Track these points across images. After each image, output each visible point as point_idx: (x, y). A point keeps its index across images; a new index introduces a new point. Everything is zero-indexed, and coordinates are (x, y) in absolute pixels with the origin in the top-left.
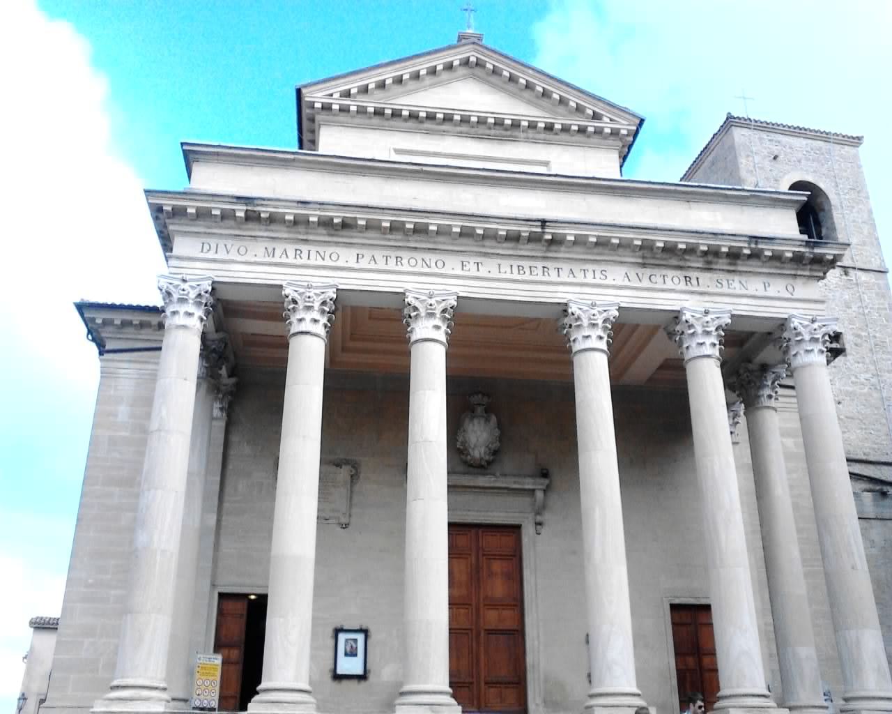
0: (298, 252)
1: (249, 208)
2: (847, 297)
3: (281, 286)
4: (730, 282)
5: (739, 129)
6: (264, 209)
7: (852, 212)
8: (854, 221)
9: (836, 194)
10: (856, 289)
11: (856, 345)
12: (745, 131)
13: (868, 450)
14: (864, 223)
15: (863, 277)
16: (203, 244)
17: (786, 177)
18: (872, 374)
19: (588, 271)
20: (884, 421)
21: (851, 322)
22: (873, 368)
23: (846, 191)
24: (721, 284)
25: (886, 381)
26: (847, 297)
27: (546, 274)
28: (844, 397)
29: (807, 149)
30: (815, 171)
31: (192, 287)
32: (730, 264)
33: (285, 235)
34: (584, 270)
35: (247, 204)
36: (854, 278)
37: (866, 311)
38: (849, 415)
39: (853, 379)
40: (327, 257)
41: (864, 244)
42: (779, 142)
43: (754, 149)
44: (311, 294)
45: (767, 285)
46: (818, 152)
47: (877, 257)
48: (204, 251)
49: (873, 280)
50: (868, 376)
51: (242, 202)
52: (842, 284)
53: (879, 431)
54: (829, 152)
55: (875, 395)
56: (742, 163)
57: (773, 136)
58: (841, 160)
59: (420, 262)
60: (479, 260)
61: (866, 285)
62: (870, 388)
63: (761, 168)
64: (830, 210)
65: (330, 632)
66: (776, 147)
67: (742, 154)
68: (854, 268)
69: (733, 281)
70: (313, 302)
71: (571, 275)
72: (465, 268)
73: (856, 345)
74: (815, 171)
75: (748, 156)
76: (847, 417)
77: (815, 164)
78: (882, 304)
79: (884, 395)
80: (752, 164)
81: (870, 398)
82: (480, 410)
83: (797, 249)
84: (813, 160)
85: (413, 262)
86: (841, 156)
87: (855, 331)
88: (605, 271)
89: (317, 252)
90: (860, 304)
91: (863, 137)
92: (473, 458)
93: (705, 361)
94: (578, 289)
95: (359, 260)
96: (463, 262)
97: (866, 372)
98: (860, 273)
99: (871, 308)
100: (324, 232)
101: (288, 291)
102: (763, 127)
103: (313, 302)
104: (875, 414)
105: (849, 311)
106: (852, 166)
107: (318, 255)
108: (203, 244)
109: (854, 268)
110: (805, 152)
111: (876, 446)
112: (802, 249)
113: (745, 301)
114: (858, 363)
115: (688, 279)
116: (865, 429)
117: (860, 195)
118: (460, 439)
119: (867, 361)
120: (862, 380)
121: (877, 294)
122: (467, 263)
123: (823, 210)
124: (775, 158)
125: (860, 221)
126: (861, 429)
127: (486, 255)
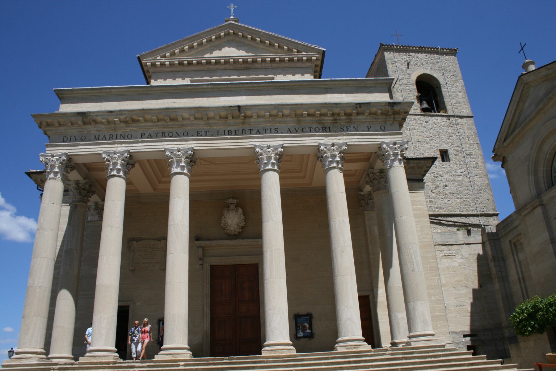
0: (111, 136)
9: (443, 79)
10: (455, 126)
11: (456, 155)
13: (462, 209)
14: (460, 92)
15: (460, 120)
16: (64, 137)
17: (415, 73)
18: (465, 170)
19: (267, 129)
20: (471, 193)
21: (453, 143)
23: (449, 77)
24: (343, 129)
26: (450, 131)
28: (449, 182)
29: (426, 57)
30: (431, 68)
32: (348, 119)
34: (265, 129)
36: (454, 121)
37: (461, 138)
38: (452, 192)
39: (454, 173)
42: (411, 56)
43: (396, 60)
45: (369, 127)
47: (467, 109)
48: (64, 141)
51: (80, 115)
52: (447, 124)
53: (468, 198)
55: (466, 180)
56: (389, 68)
58: (446, 61)
59: (175, 134)
61: (461, 124)
62: (463, 177)
63: (401, 70)
66: (409, 58)
67: (389, 63)
68: (454, 116)
69: (350, 127)
71: (258, 132)
73: (456, 155)
75: (393, 64)
76: (450, 193)
77: (431, 65)
78: (470, 133)
79: (471, 179)
80: (395, 68)
81: (464, 182)
87: (455, 148)
88: (277, 129)
90: (457, 134)
93: (332, 171)
95: (143, 136)
96: (198, 132)
98: (457, 119)
106: (452, 64)
107: (121, 136)
108: (64, 137)
109: (454, 116)
110: (425, 59)
111: (466, 206)
114: (457, 164)
116: (461, 198)
117: (457, 78)
119: (462, 163)
120: (459, 173)
121: (467, 128)
122: (200, 132)
124: (408, 64)
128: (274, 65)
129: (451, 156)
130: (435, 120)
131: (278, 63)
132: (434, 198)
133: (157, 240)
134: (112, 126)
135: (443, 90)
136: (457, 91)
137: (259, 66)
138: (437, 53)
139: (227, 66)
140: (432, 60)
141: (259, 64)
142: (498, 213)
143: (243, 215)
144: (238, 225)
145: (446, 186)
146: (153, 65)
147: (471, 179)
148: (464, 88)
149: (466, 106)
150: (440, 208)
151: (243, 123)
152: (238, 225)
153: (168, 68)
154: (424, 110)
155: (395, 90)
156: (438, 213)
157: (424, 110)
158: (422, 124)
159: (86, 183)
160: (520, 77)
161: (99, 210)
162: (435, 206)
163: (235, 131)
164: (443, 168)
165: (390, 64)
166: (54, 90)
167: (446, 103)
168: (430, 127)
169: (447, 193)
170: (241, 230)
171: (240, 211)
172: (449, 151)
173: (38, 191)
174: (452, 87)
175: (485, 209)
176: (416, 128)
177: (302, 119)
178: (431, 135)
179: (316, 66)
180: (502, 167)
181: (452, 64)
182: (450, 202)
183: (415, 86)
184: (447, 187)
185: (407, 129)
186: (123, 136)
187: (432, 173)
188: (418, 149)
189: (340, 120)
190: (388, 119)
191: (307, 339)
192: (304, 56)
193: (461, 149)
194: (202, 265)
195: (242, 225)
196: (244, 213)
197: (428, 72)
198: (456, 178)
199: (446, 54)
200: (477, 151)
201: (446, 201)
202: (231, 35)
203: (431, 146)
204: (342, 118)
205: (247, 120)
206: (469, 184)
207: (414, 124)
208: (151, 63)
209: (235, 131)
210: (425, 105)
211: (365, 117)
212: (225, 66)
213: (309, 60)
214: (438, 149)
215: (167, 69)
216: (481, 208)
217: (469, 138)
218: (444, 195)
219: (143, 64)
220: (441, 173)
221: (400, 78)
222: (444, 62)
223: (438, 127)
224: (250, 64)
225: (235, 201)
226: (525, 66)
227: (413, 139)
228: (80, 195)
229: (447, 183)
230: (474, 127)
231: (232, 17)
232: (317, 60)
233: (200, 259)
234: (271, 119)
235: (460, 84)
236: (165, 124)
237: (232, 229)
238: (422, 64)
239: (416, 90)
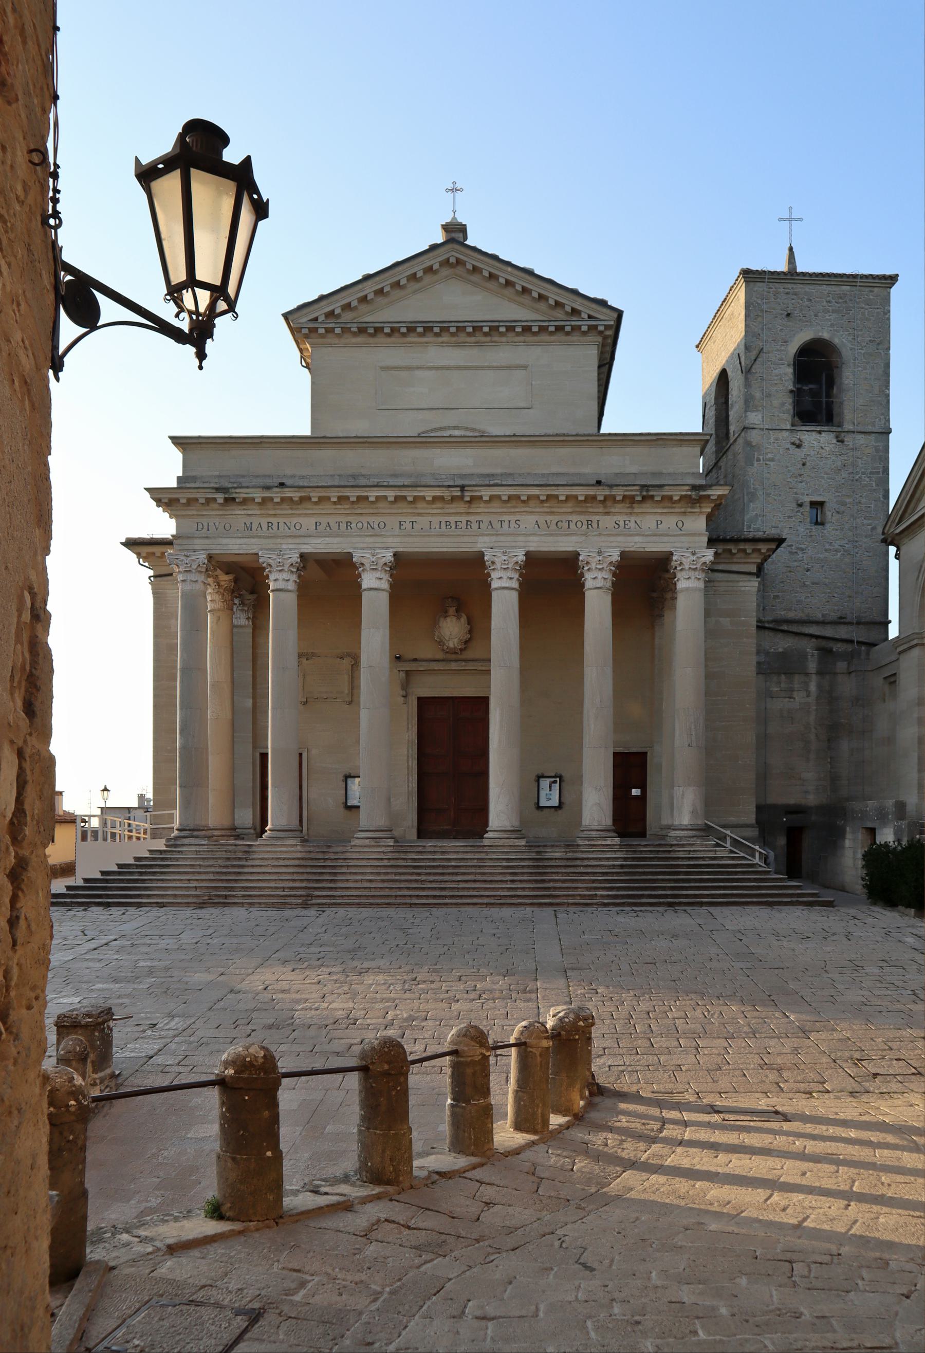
1: (227, 496)
4: (627, 522)
6: (237, 495)
25: (861, 546)
27: (469, 527)
33: (258, 512)
35: (224, 493)
40: (292, 528)
46: (841, 301)
59: (365, 525)
60: (414, 519)
65: (341, 778)
70: (283, 566)
71: (490, 527)
72: (402, 527)
82: (452, 610)
83: (684, 493)
84: (834, 311)
85: (360, 525)
91: (897, 275)
92: (448, 647)
100: (288, 507)
102: (780, 279)
110: (825, 303)
112: (689, 493)
115: (590, 522)
117: (880, 347)
118: (437, 634)
127: (419, 514)
130: (815, 442)
140: (839, 305)
158: (788, 449)
163: (456, 522)
174: (865, 369)
181: (877, 313)
183: (792, 366)
185: (758, 460)
186: (289, 525)
187: (789, 546)
190: (689, 510)
197: (826, 335)
209: (456, 522)
222: (863, 308)
223: (819, 456)
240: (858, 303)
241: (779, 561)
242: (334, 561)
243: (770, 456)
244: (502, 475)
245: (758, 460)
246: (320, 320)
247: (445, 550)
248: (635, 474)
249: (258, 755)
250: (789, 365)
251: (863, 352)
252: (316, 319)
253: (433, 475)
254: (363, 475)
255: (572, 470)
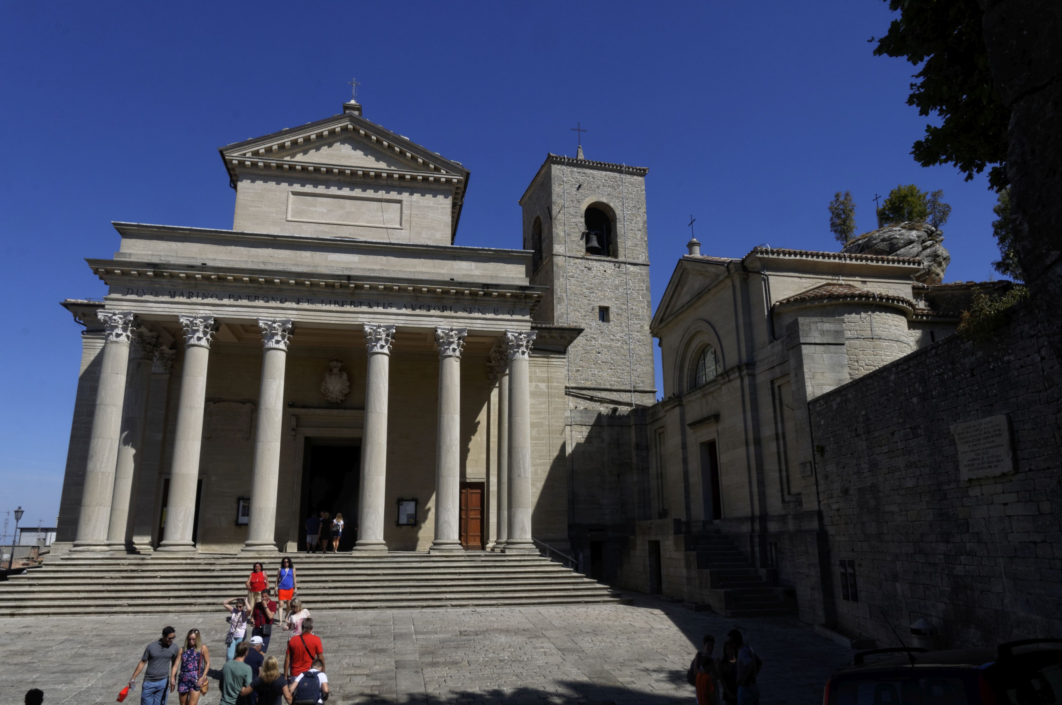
2: (617, 282)
3: (178, 316)
5: (556, 165)
7: (631, 223)
8: (632, 230)
9: (621, 210)
11: (618, 315)
12: (559, 167)
14: (639, 230)
15: (631, 268)
17: (587, 199)
20: (628, 363)
21: (617, 299)
22: (627, 329)
26: (617, 282)
30: (608, 195)
31: (120, 318)
36: (624, 270)
37: (629, 292)
38: (605, 360)
39: (612, 337)
41: (636, 245)
44: (197, 322)
49: (638, 270)
50: (622, 335)
53: (624, 370)
54: (621, 180)
55: (625, 347)
57: (580, 170)
58: (630, 186)
63: (568, 193)
64: (616, 222)
68: (625, 263)
73: (618, 315)
74: (608, 195)
75: (561, 184)
77: (609, 189)
78: (642, 287)
79: (631, 347)
80: (562, 191)
86: (631, 183)
87: (619, 305)
89: (203, 294)
90: (625, 287)
94: (372, 316)
97: (622, 332)
98: (628, 266)
99: (633, 290)
101: (183, 320)
103: (199, 327)
104: (622, 359)
105: (617, 292)
109: (625, 263)
111: (619, 380)
113: (479, 321)
117: (640, 211)
119: (624, 324)
120: (618, 337)
121: (639, 280)
123: (613, 221)
124: (580, 186)
125: (636, 229)
126: (611, 369)
128: (403, 184)
129: (611, 316)
131: (408, 181)
132: (582, 367)
133: (241, 402)
134: (193, 282)
135: (619, 226)
136: (636, 229)
137: (384, 182)
138: (621, 172)
139: (341, 178)
141: (384, 180)
142: (655, 390)
143: (349, 381)
144: (341, 392)
145: (599, 353)
146: (241, 163)
147: (631, 347)
148: (646, 226)
149: (644, 251)
150: (587, 380)
151: (352, 294)
152: (341, 392)
153: (261, 170)
154: (590, 250)
155: (557, 223)
156: (583, 386)
157: (590, 250)
159: (152, 337)
160: (680, 260)
161: (165, 361)
162: (582, 377)
164: (600, 330)
165: (557, 185)
166: (113, 223)
167: (619, 244)
168: (593, 275)
169: (599, 362)
170: (344, 398)
171: (345, 376)
172: (611, 309)
173: (77, 324)
175: (641, 385)
176: (576, 275)
177: (420, 295)
178: (593, 286)
179: (457, 188)
180: (660, 345)
182: (600, 373)
184: (599, 355)
185: (563, 276)
188: (573, 304)
189: (463, 299)
191: (410, 527)
192: (443, 176)
193: (626, 307)
194: (294, 436)
195: (345, 392)
196: (350, 379)
197: (604, 200)
198: (614, 344)
199: (632, 174)
200: (645, 310)
201: (596, 372)
202: (350, 131)
203: (589, 300)
204: (466, 297)
205: (357, 291)
206: (627, 353)
207: (573, 271)
208: (238, 160)
210: (595, 243)
211: (492, 299)
212: (338, 178)
213: (449, 181)
214: (598, 305)
215: (259, 172)
216: (637, 383)
217: (638, 294)
218: (594, 364)
219: (227, 161)
220: (595, 336)
221: (566, 206)
224: (372, 178)
225: (339, 365)
226: (691, 245)
227: (568, 291)
228: (144, 350)
229: (601, 349)
230: (648, 279)
231: (353, 102)
232: (459, 181)
233: (293, 430)
234: (385, 293)
235: (641, 219)
236: (259, 286)
237: (334, 396)
238: (598, 188)
239: (584, 224)
240: (625, 183)
241: (579, 345)
242: (242, 326)
243: (570, 274)
244: (380, 270)
245: (563, 276)
246: (247, 155)
247: (333, 322)
248: (479, 276)
249: (163, 482)
250: (582, 217)
251: (629, 213)
252: (245, 154)
253: (327, 267)
254: (270, 263)
255: (433, 271)
